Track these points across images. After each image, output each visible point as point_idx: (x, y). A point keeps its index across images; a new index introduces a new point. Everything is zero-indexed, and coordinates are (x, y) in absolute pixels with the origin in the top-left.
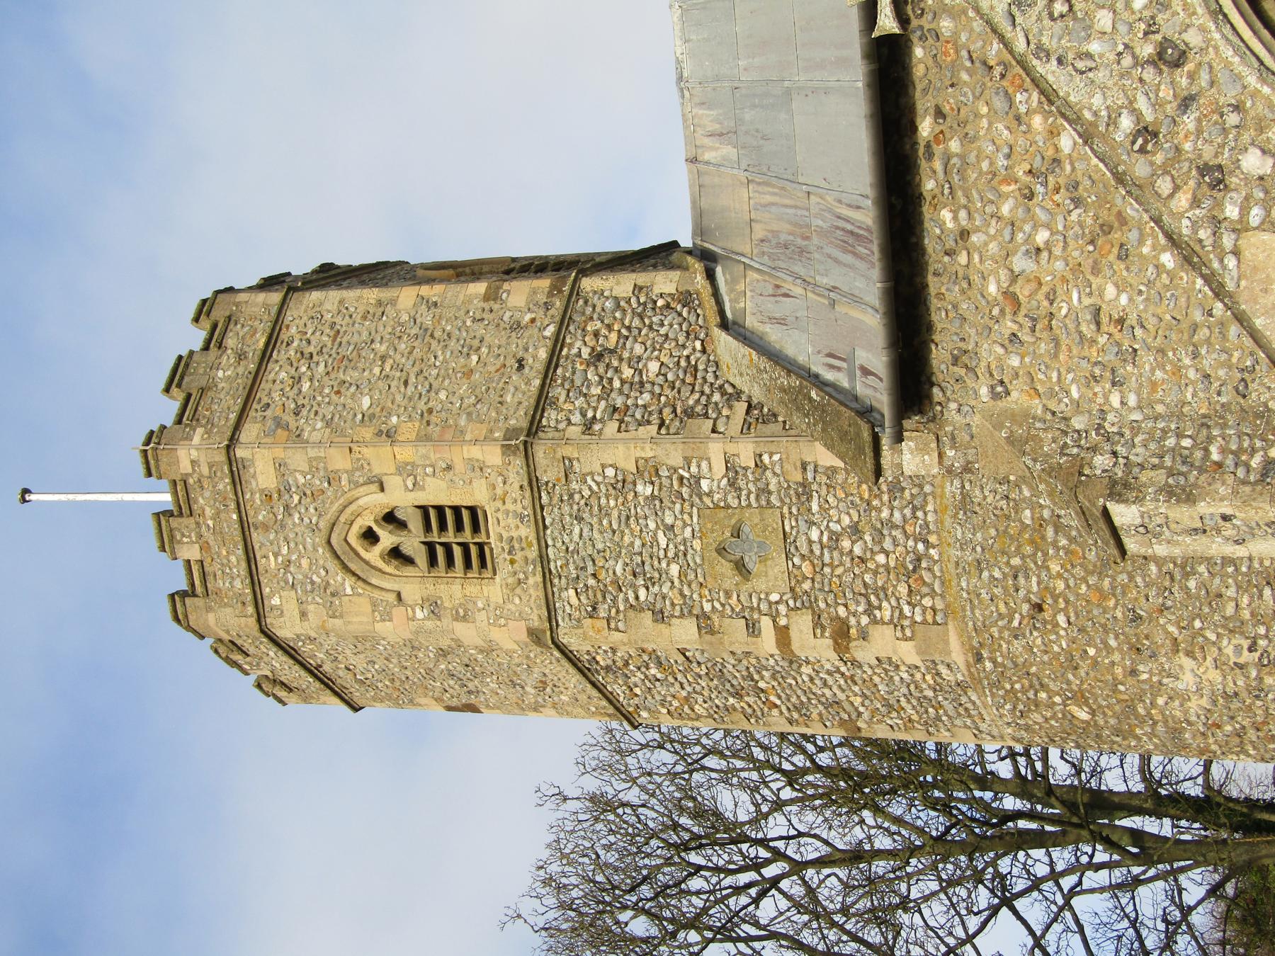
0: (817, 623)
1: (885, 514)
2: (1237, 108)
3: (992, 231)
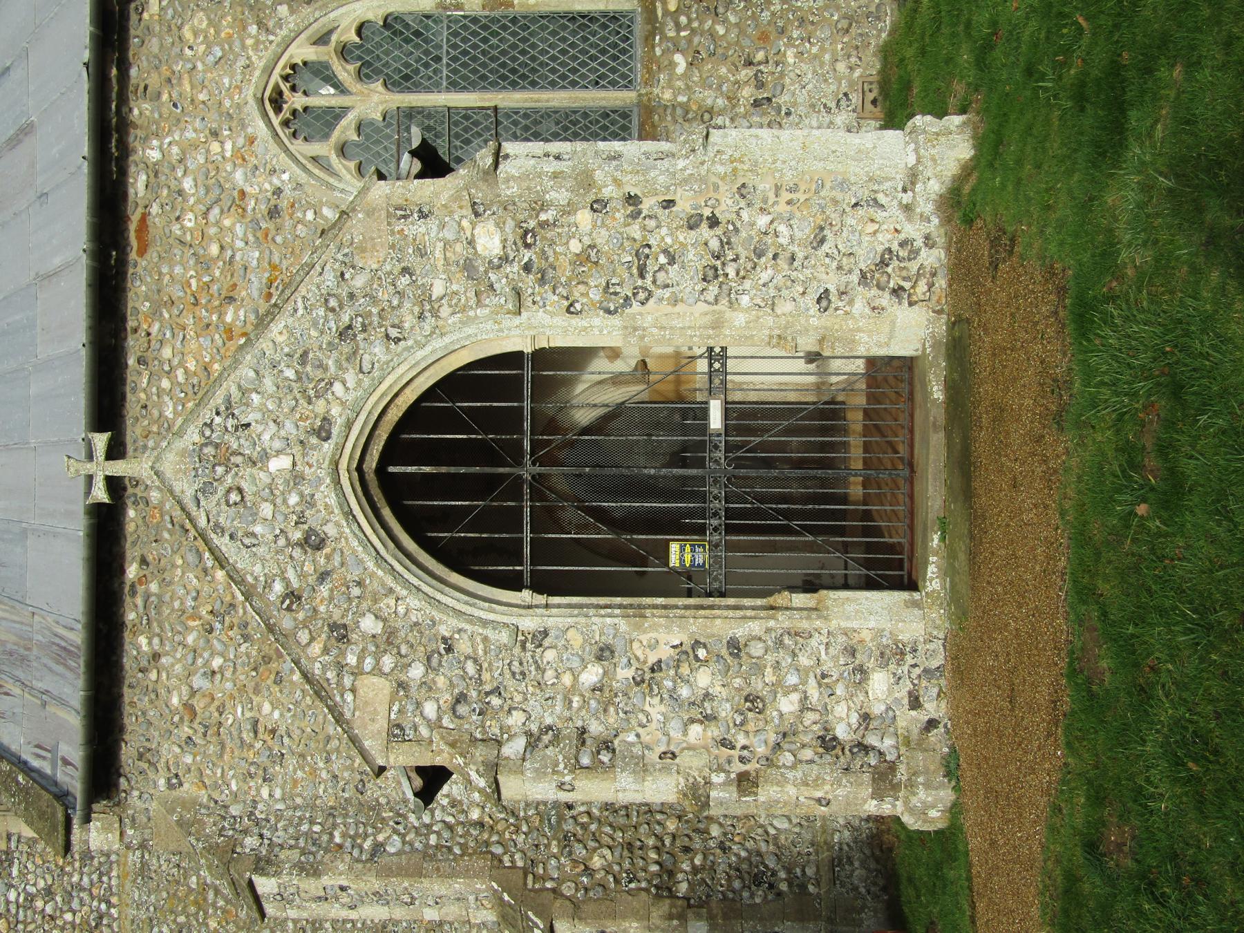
1: (75, 879)
2: (359, 584)
3: (178, 656)
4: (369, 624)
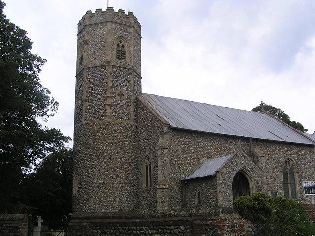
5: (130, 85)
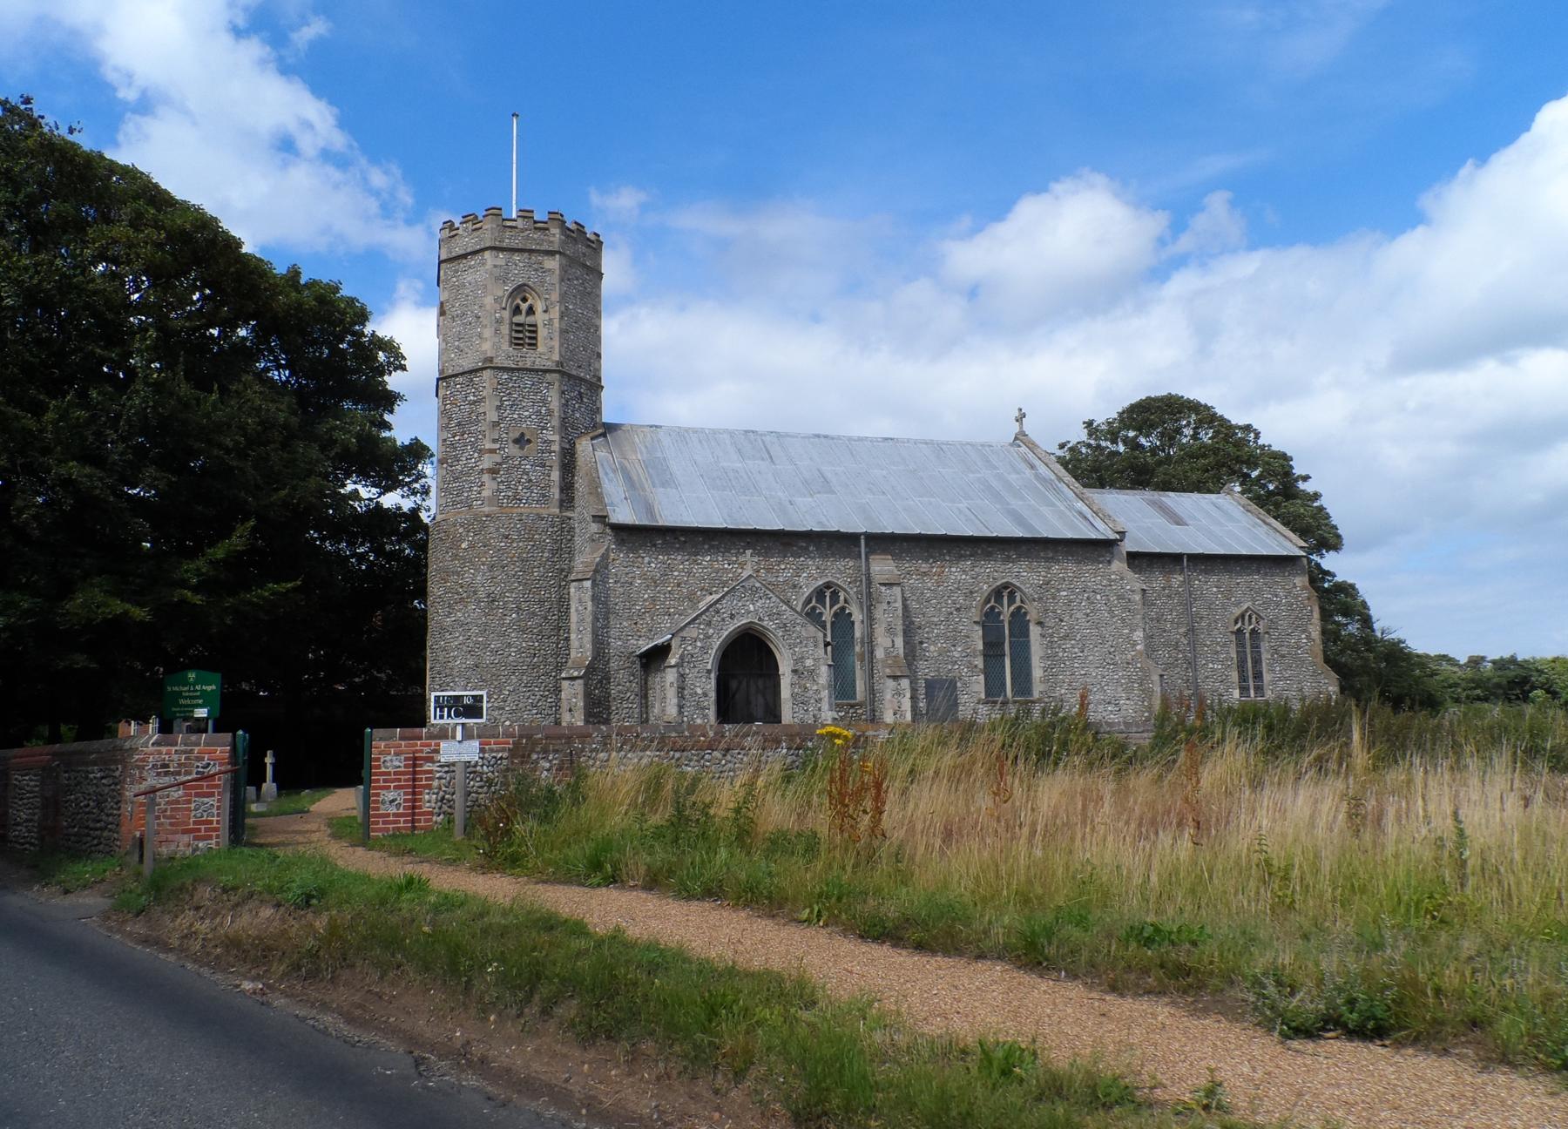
0: (497, 463)
4: (711, 631)
5: (550, 413)
